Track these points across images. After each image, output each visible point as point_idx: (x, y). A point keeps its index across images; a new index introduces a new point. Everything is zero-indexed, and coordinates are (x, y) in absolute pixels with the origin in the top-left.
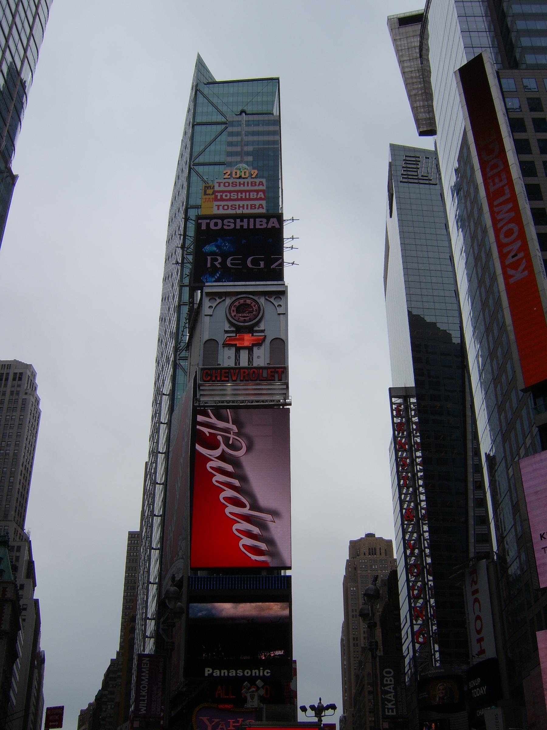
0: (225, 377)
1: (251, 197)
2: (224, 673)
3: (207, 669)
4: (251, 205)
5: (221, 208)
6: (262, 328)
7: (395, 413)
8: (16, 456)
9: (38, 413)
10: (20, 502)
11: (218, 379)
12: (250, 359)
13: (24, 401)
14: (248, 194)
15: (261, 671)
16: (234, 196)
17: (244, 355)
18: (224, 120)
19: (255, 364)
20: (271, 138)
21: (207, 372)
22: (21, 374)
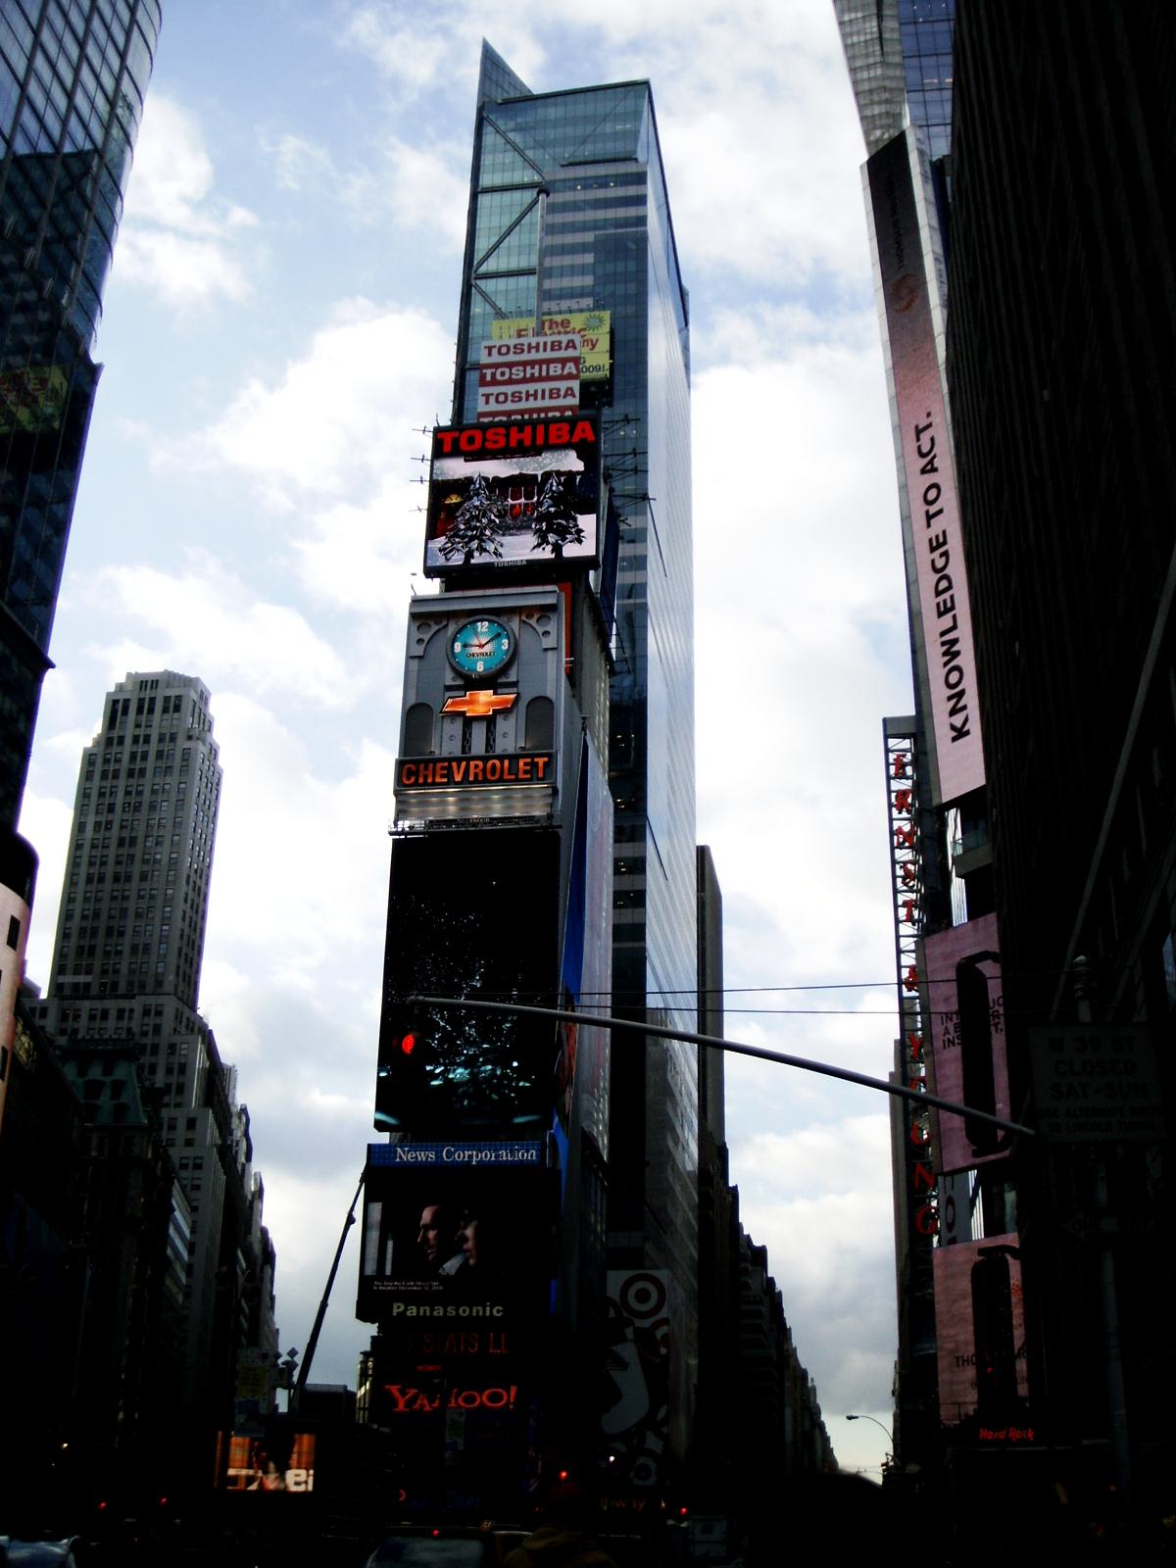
0: (442, 776)
1: (551, 373)
2: (425, 1311)
3: (395, 1306)
4: (551, 390)
5: (492, 399)
6: (513, 678)
7: (893, 769)
8: (174, 864)
9: (217, 775)
10: (186, 955)
11: (430, 780)
12: (490, 743)
13: (187, 756)
14: (544, 367)
15: (488, 1308)
16: (518, 373)
17: (479, 733)
18: (537, 178)
19: (498, 751)
20: (632, 212)
21: (409, 769)
22: (179, 698)
